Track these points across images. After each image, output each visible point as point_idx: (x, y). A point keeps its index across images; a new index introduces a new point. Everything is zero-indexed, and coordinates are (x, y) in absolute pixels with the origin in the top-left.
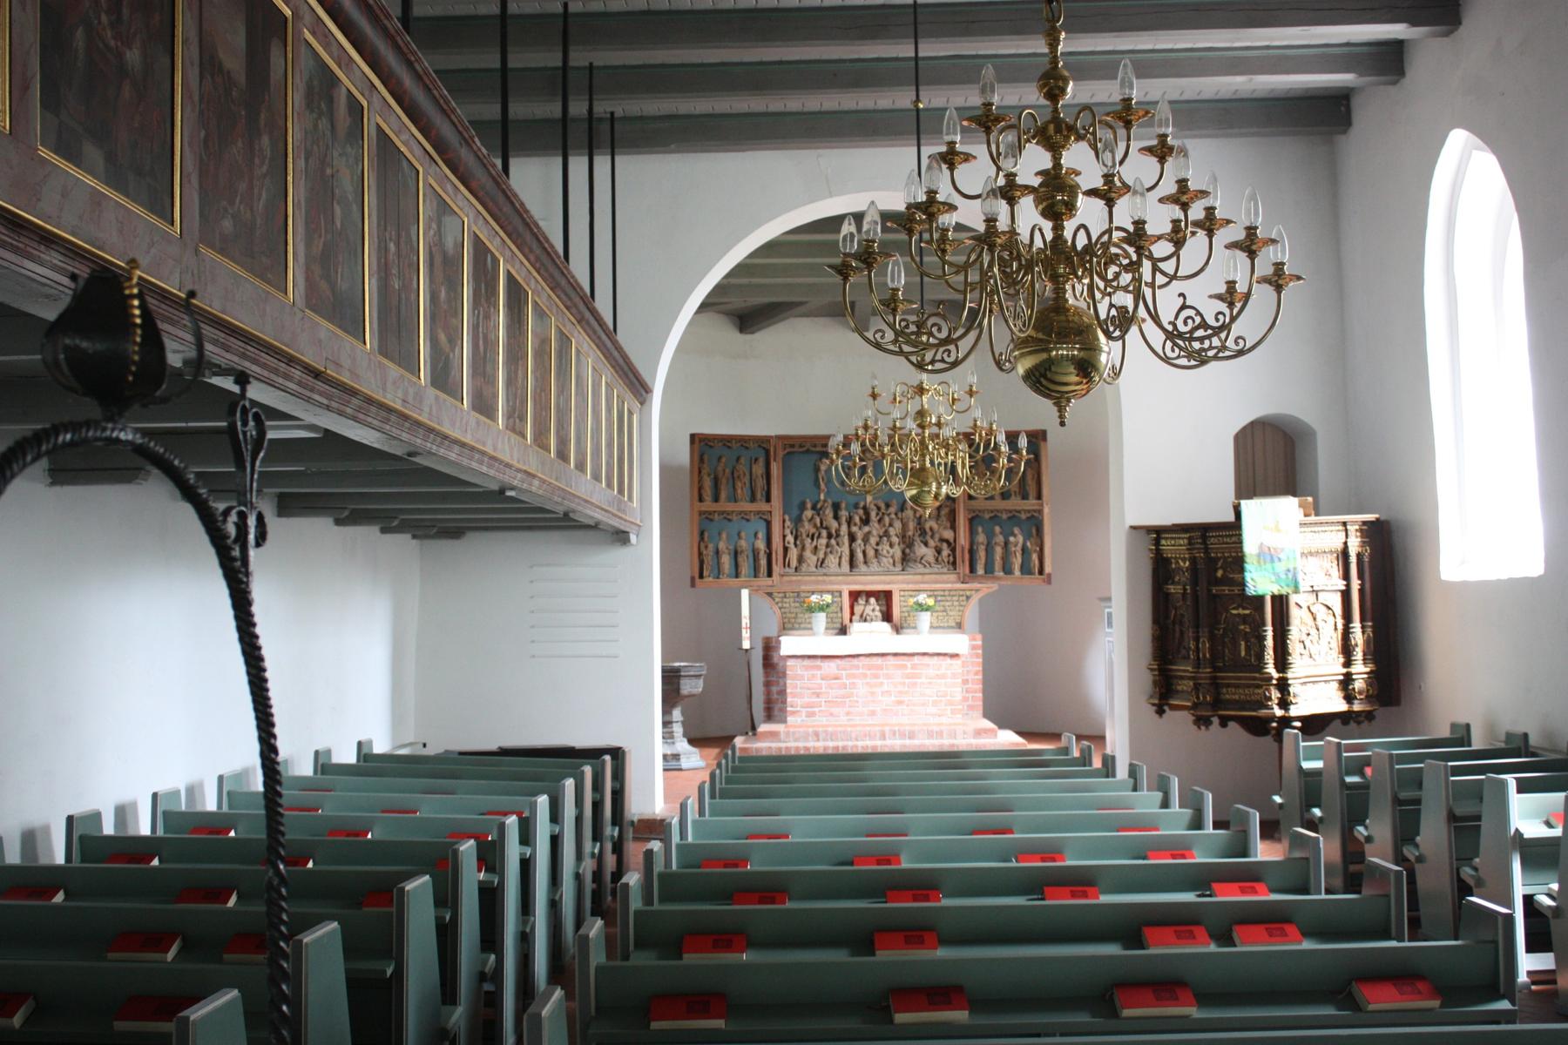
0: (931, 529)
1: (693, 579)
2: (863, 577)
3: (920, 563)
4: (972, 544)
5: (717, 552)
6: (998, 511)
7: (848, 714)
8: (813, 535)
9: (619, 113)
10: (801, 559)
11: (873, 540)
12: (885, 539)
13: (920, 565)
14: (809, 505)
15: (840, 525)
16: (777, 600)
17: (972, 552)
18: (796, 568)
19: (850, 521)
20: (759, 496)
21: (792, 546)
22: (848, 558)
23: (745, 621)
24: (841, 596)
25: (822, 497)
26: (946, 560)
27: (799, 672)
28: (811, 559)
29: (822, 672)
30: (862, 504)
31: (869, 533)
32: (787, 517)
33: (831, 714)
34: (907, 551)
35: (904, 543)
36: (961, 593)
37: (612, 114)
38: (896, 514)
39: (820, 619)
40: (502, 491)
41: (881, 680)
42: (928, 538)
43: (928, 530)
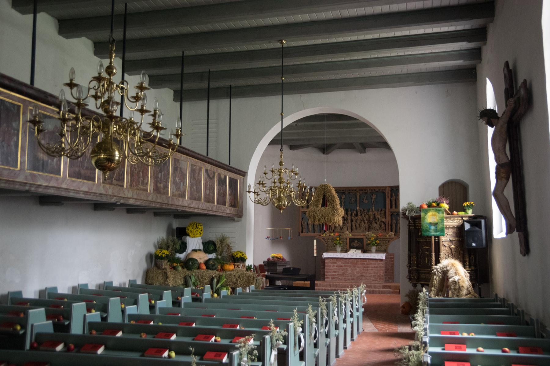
0: (378, 218)
1: (299, 233)
4: (391, 223)
5: (308, 224)
6: (393, 212)
7: (345, 279)
9: (233, 85)
11: (358, 222)
12: (363, 221)
13: (374, 230)
15: (348, 216)
16: (326, 240)
17: (391, 226)
18: (334, 230)
19: (351, 215)
22: (350, 227)
23: (315, 247)
24: (346, 240)
26: (383, 229)
27: (329, 264)
29: (337, 264)
33: (339, 278)
34: (370, 225)
35: (369, 222)
36: (387, 240)
37: (231, 85)
38: (367, 213)
39: (339, 249)
40: (116, 203)
41: (356, 268)
42: (377, 221)
43: (377, 219)
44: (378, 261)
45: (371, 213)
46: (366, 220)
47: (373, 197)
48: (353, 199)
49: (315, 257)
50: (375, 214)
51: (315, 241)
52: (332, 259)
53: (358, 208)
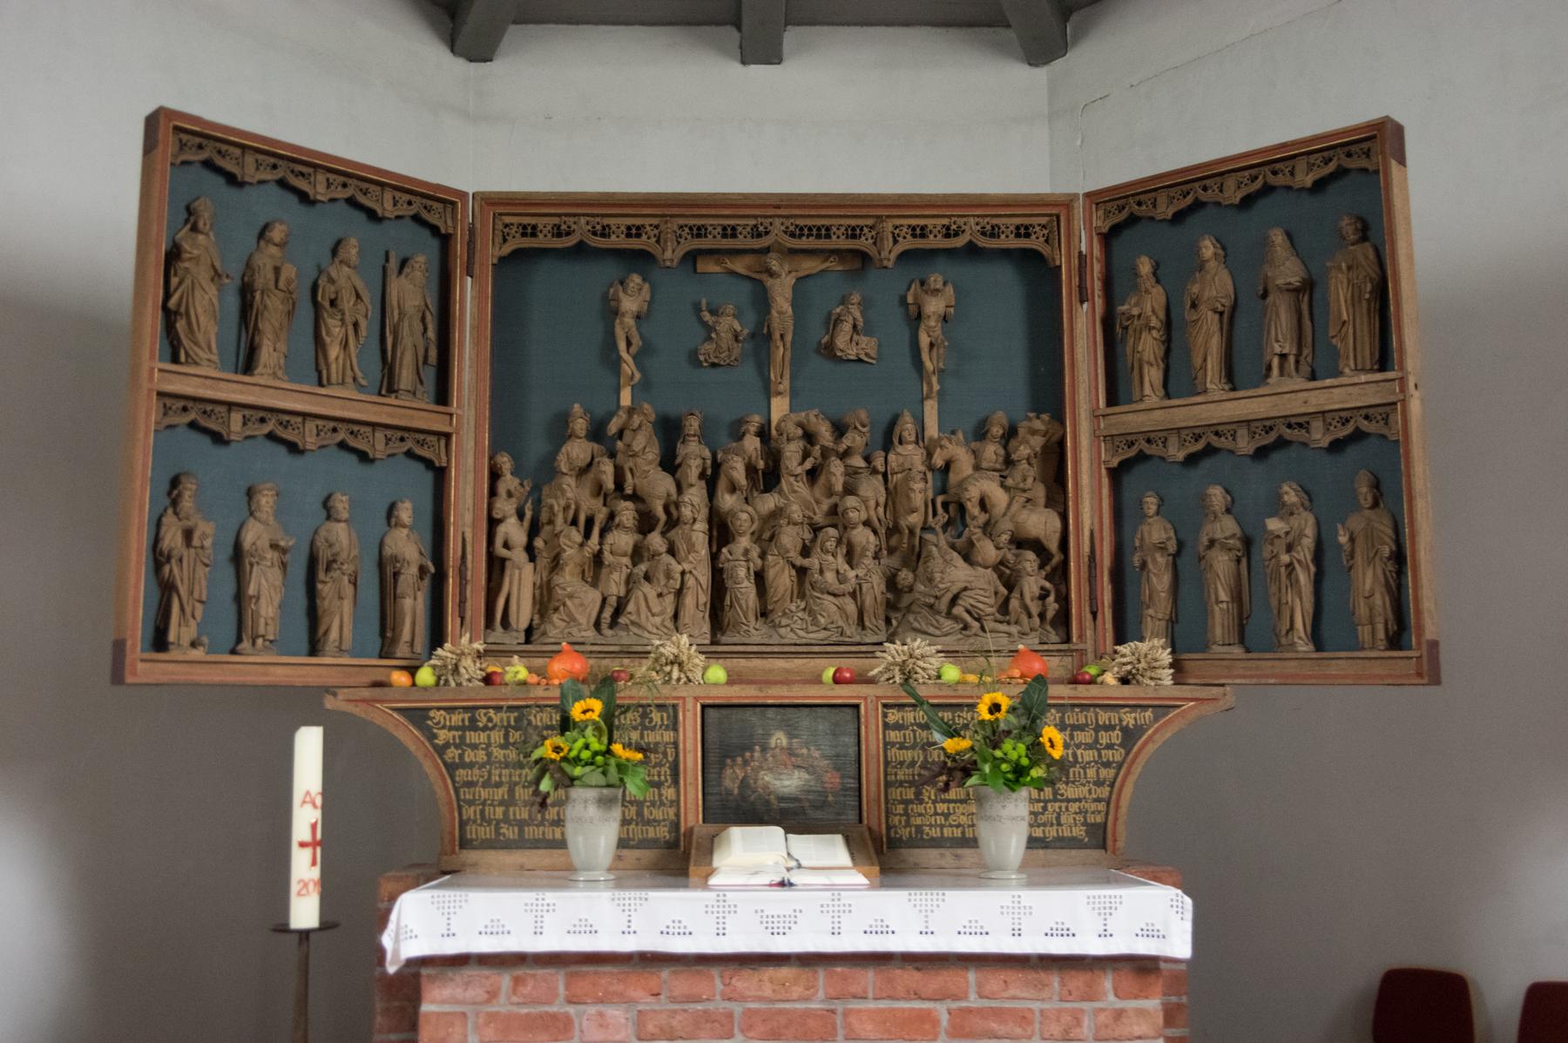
0: (983, 504)
2: (757, 663)
3: (949, 615)
8: (590, 522)
10: (545, 601)
11: (790, 538)
12: (832, 532)
13: (948, 624)
14: (580, 425)
16: (443, 736)
18: (529, 632)
19: (711, 479)
20: (406, 377)
21: (518, 555)
22: (704, 598)
23: (305, 819)
24: (674, 726)
25: (626, 398)
28: (582, 600)
30: (756, 420)
31: (777, 513)
32: (505, 462)
34: (905, 576)
35: (891, 551)
36: (1104, 717)
38: (867, 459)
44: (1107, 982)
45: (909, 455)
46: (867, 523)
47: (934, 306)
48: (727, 324)
49: (305, 934)
50: (948, 466)
51: (309, 745)
52: (505, 980)
53: (779, 407)
